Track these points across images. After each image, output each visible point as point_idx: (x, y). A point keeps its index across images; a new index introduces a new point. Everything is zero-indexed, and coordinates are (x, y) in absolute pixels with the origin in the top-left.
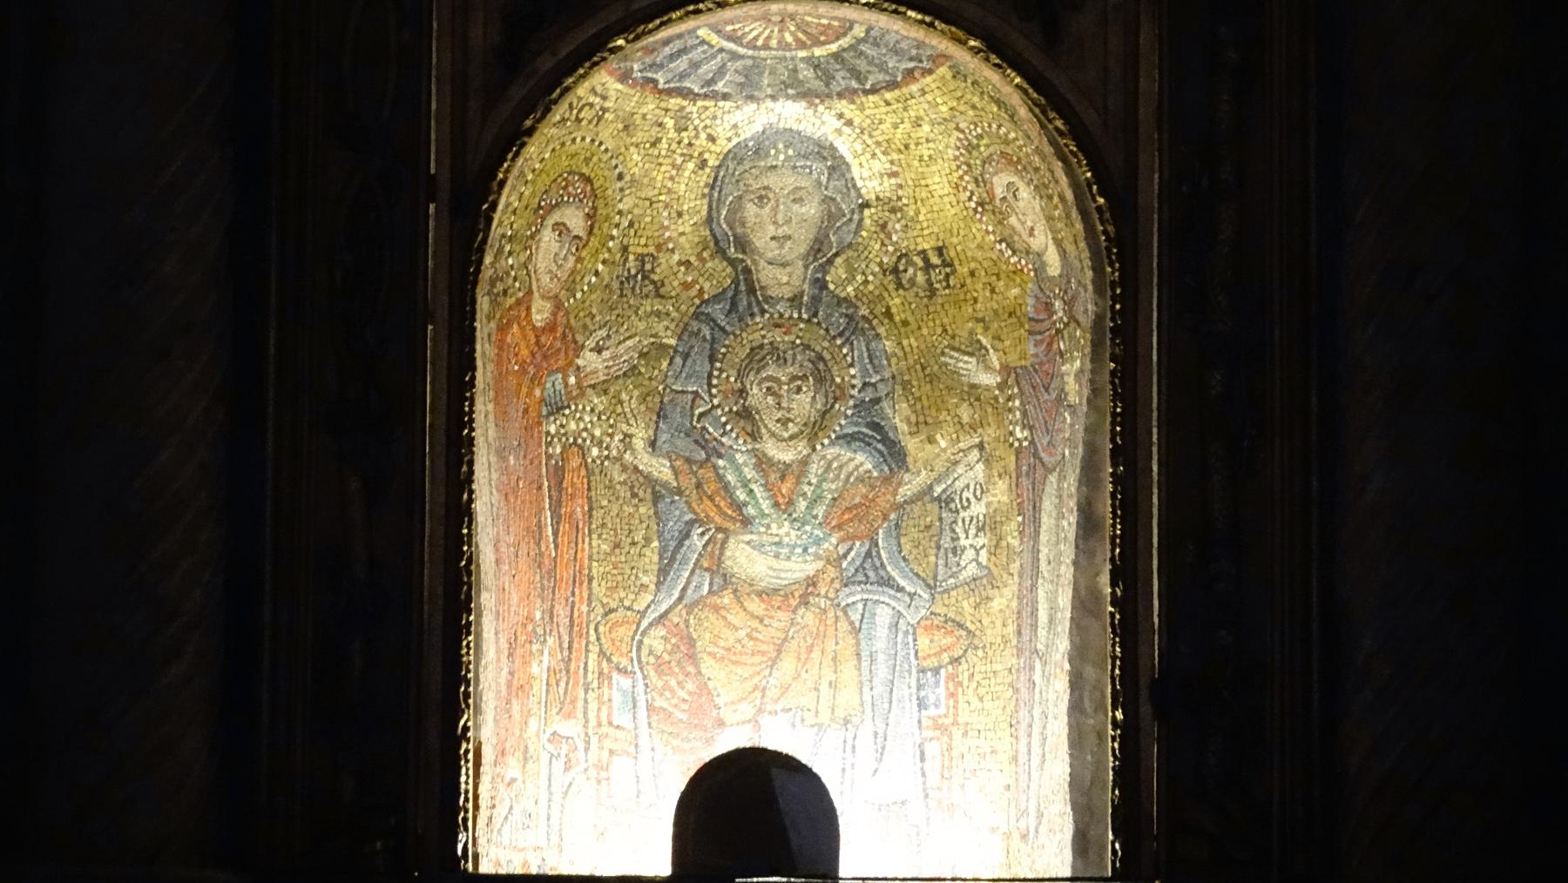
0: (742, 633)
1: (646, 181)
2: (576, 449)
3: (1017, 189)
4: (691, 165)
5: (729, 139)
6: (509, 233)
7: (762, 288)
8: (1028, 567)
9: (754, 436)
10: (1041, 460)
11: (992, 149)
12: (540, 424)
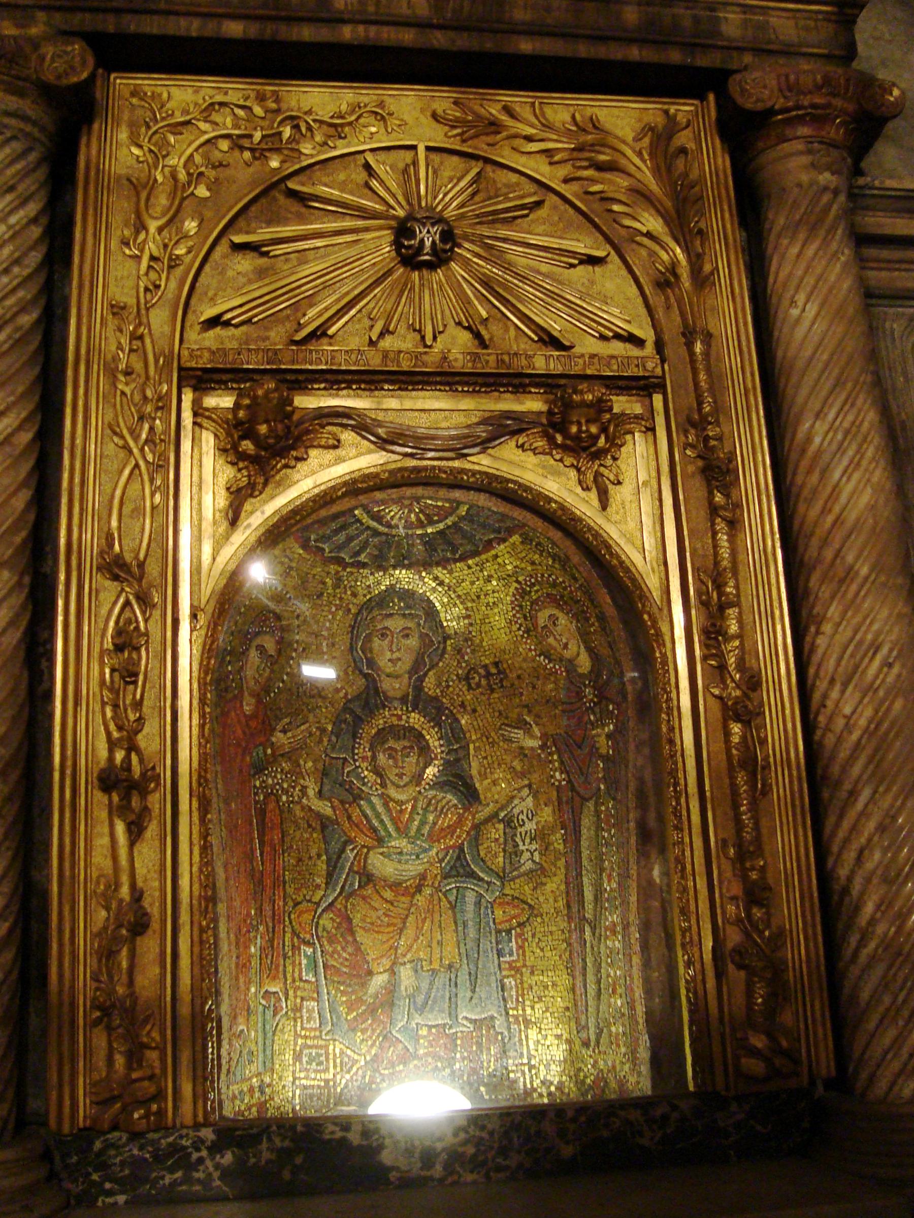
0: (381, 913)
4: (341, 613)
5: (365, 596)
9: (383, 785)
10: (578, 793)
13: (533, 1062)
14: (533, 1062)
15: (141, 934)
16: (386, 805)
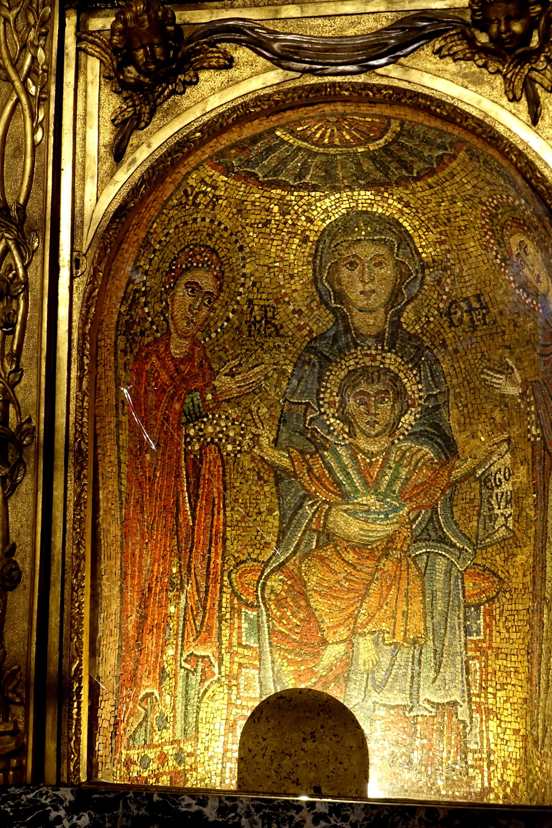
1: (262, 252)
2: (213, 446)
3: (526, 247)
4: (297, 241)
5: (323, 221)
6: (143, 289)
7: (355, 329)
8: (540, 532)
11: (506, 216)
12: (180, 429)
13: (492, 758)
14: (492, 758)
15: (12, 588)
16: (353, 457)
